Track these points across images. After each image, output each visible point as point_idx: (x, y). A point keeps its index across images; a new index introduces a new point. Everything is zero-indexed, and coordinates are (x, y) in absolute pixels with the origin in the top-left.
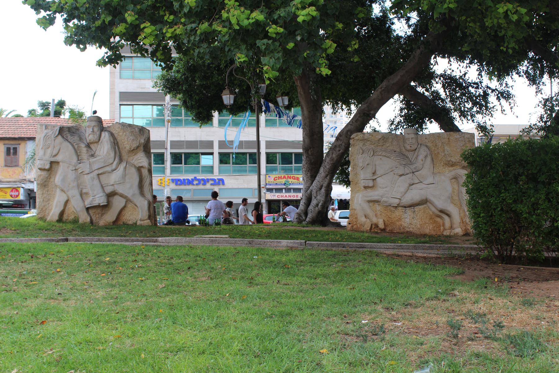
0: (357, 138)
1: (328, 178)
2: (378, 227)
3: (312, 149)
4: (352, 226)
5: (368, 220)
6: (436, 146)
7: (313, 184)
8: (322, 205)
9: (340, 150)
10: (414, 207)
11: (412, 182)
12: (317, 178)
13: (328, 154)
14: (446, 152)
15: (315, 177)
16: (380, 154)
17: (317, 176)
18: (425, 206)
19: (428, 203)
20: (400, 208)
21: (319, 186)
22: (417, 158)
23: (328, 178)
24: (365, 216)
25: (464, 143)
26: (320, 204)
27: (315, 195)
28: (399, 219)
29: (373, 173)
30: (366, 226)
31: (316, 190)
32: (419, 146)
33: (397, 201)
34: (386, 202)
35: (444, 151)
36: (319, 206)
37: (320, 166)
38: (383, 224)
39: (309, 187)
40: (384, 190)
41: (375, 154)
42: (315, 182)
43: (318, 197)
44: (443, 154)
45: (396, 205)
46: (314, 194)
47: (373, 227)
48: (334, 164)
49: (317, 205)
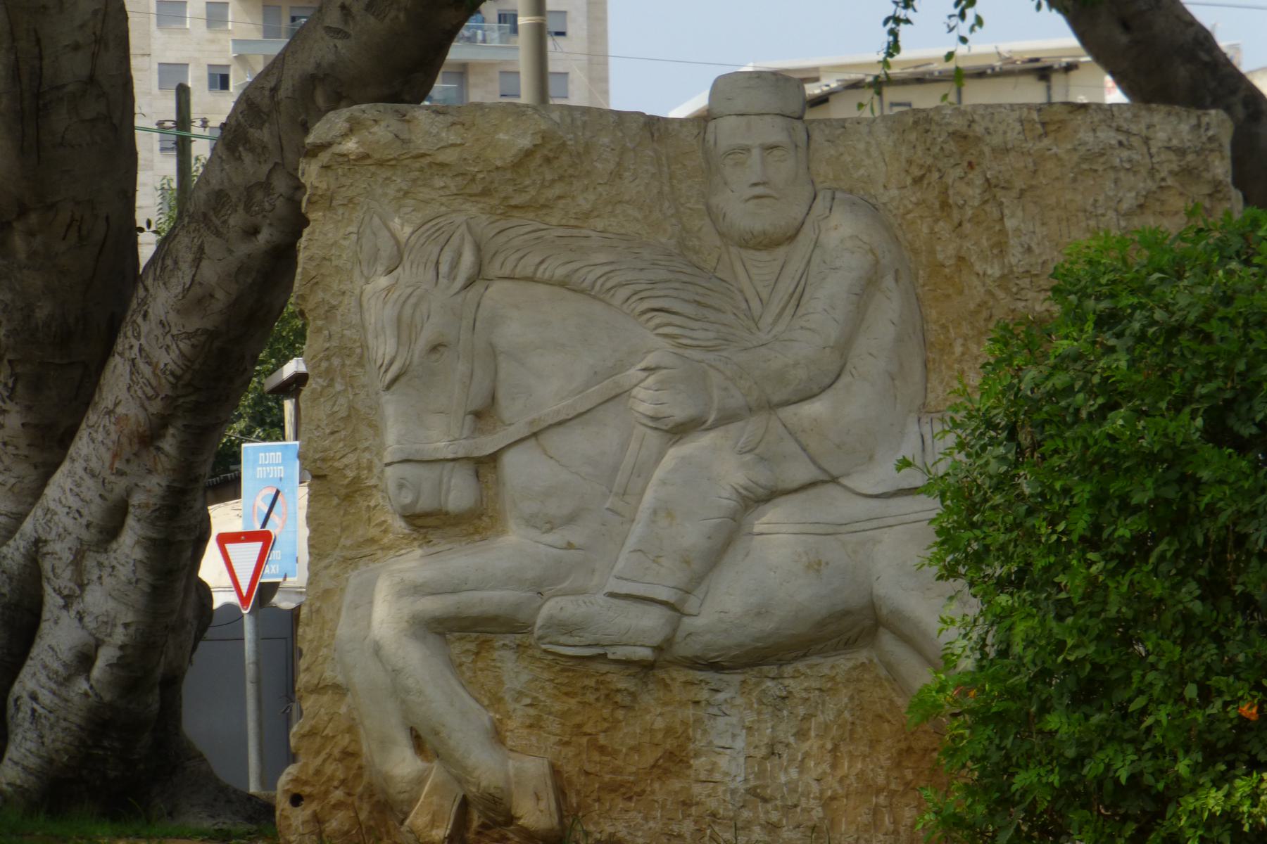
0: (351, 145)
1: (169, 444)
2: (510, 819)
3: (33, 218)
4: (318, 820)
5: (436, 772)
6: (945, 205)
7: (51, 491)
8: (120, 664)
9: (254, 232)
10: (781, 663)
11: (763, 477)
12: (82, 446)
13: (153, 261)
14: (1015, 256)
15: (69, 435)
16: (527, 266)
17: (83, 433)
18: (862, 656)
19: (887, 642)
20: (680, 675)
21: (95, 511)
22: (797, 298)
23: (169, 444)
24: (418, 742)
25: (1144, 184)
26: (105, 656)
27: (65, 579)
28: (670, 755)
29: (478, 415)
30: (418, 818)
31: (70, 542)
32: (820, 205)
33: (651, 622)
34: (566, 628)
35: (1000, 248)
36: (99, 669)
37: (107, 351)
38: (549, 802)
39: (19, 518)
40: (556, 537)
41: (494, 269)
42: (61, 480)
43: (97, 600)
44: (995, 271)
45: (644, 653)
46: (57, 576)
47: (476, 820)
48: (212, 335)
49: (85, 660)
